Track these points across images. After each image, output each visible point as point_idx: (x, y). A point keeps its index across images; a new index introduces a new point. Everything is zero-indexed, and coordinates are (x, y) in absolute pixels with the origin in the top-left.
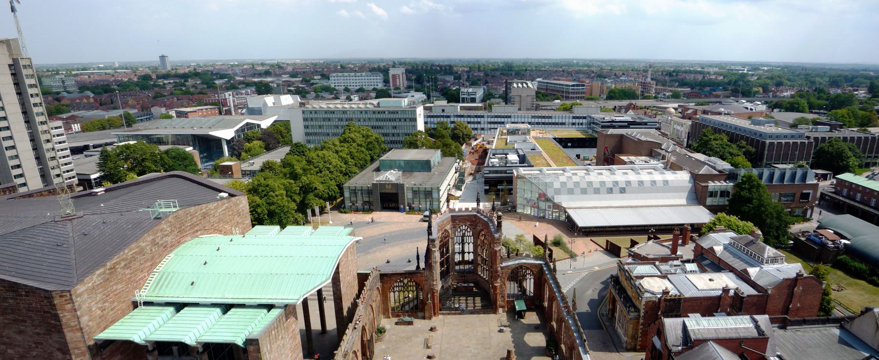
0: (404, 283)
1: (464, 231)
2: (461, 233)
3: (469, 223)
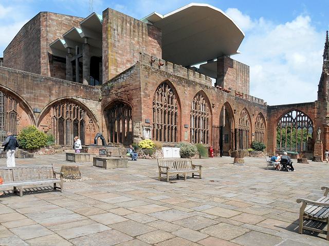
0: (292, 118)
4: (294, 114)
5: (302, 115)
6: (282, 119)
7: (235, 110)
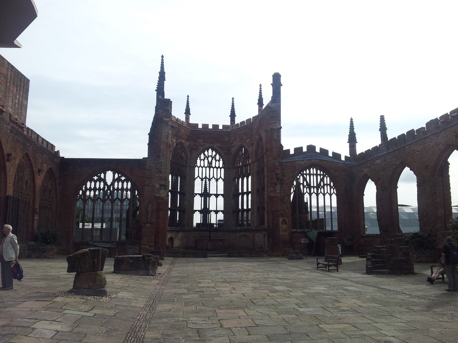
0: (105, 184)
1: (210, 159)
2: (206, 161)
3: (219, 145)
4: (109, 176)
5: (123, 178)
6: (88, 183)
7: (9, 155)
